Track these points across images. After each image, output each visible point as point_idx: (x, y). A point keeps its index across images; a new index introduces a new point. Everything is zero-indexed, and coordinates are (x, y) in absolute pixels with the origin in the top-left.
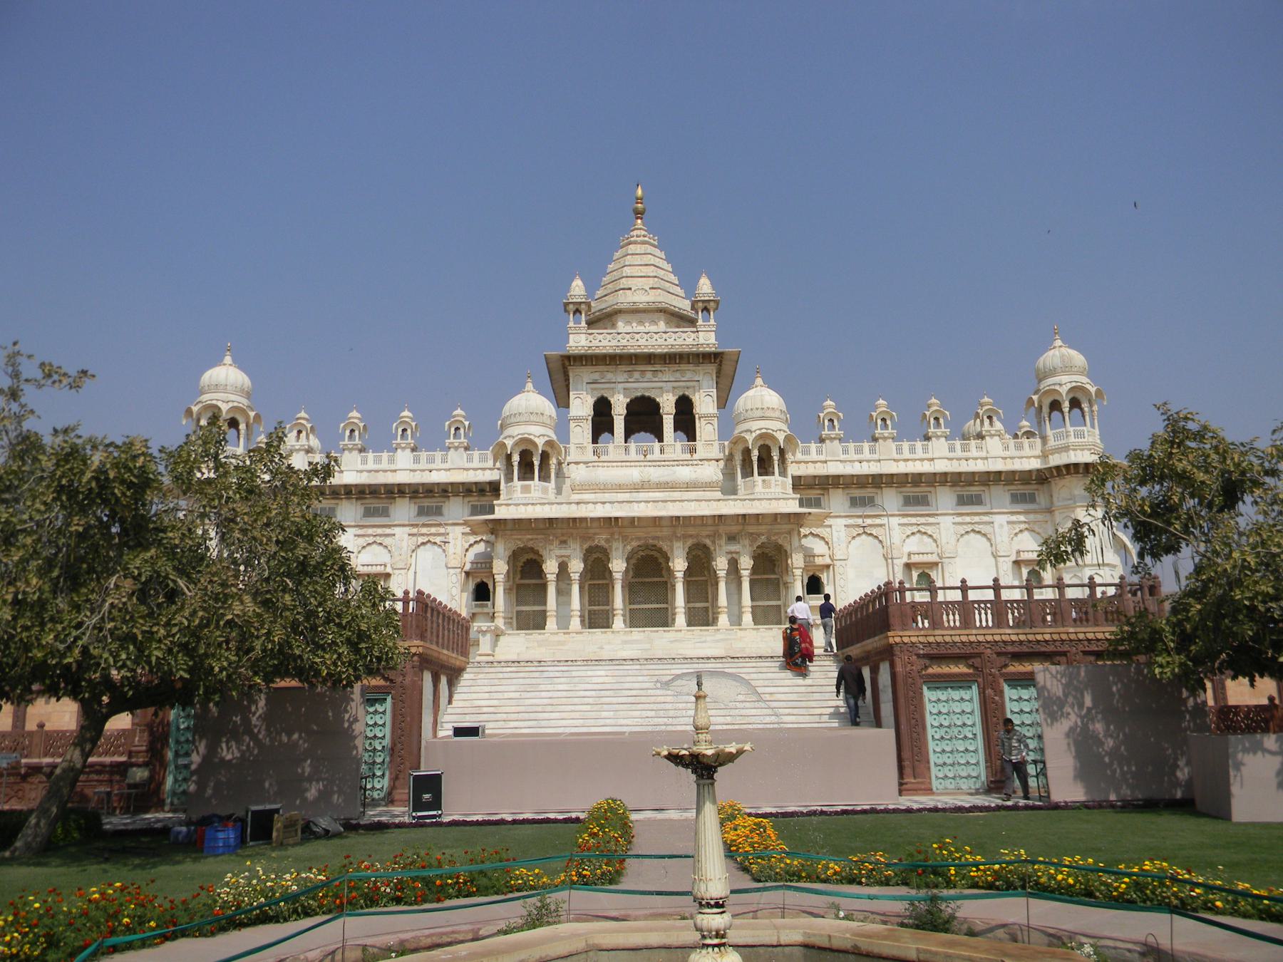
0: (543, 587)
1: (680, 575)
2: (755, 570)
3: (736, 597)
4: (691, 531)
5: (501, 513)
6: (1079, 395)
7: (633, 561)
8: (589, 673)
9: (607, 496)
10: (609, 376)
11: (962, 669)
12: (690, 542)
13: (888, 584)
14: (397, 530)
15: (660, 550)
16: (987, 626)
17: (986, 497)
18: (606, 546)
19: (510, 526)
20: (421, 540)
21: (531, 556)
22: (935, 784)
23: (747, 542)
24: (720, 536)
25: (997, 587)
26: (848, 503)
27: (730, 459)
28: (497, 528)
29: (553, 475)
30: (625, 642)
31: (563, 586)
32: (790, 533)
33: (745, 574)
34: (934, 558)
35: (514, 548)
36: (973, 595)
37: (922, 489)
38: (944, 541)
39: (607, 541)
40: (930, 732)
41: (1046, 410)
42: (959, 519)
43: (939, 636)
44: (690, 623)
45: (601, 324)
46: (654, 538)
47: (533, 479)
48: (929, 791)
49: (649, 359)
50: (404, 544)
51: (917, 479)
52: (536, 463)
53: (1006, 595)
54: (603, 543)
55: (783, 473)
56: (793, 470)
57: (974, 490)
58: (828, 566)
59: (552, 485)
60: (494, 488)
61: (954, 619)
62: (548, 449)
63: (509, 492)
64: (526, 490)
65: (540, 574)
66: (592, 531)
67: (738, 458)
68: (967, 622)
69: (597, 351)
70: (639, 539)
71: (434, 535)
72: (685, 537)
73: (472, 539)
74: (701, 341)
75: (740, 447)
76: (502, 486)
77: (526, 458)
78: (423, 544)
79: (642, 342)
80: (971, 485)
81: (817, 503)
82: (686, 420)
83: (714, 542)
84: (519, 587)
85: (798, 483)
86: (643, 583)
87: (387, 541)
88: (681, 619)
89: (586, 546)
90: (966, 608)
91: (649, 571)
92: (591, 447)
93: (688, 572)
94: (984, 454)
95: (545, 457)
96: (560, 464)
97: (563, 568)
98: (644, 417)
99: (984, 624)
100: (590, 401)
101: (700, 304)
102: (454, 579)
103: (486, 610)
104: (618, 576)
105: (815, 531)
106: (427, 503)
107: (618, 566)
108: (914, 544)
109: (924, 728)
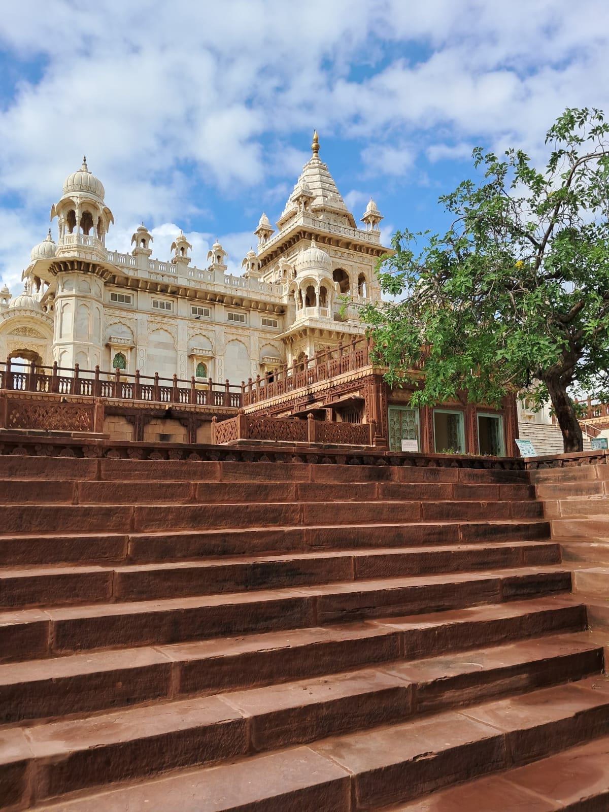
14: (217, 328)
20: (232, 337)
50: (223, 338)
87: (211, 335)
106: (235, 312)
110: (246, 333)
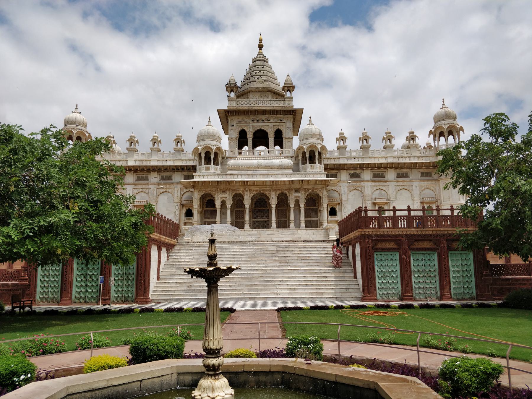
0: (216, 211)
1: (274, 206)
2: (307, 204)
3: (298, 216)
4: (279, 188)
5: (196, 179)
6: (452, 129)
7: (255, 200)
8: (231, 247)
9: (243, 172)
10: (246, 120)
11: (392, 245)
12: (278, 192)
13: (360, 208)
14: (152, 186)
15: (266, 196)
16: (404, 228)
17: (410, 174)
18: (242, 193)
19: (200, 184)
20: (162, 190)
21: (211, 198)
22: (378, 297)
23: (303, 192)
24: (291, 190)
25: (409, 210)
26: (348, 177)
27: (297, 157)
28: (195, 185)
29: (220, 163)
30: (250, 235)
31: (223, 210)
32: (322, 188)
33: (302, 206)
34: (385, 201)
35: (202, 194)
36: (398, 213)
37: (382, 170)
38: (390, 193)
39: (243, 191)
40: (377, 274)
41: (437, 135)
42: (398, 184)
43: (382, 231)
44: (278, 227)
45: (243, 97)
46: (263, 190)
47: (211, 164)
48: (376, 300)
49: (263, 112)
50: (155, 192)
51: (380, 166)
52: (212, 157)
53: (412, 213)
54: (241, 192)
55: (320, 163)
56: (325, 162)
57: (405, 171)
58: (339, 204)
59: (219, 167)
60: (194, 169)
61: (388, 224)
62: (218, 151)
63: (200, 170)
64: (208, 169)
65: (214, 205)
66: (236, 187)
67: (300, 156)
68: (395, 225)
69: (241, 108)
70: (257, 190)
71: (168, 188)
72: (276, 190)
73: (185, 190)
74: (286, 105)
75: (301, 151)
76: (198, 167)
77: (207, 154)
78: (163, 192)
79: (260, 105)
80: (402, 169)
81: (335, 176)
82: (279, 140)
83: (289, 192)
84: (205, 211)
85: (326, 168)
86: (259, 210)
88: (274, 225)
89: (234, 193)
90: (395, 219)
91: (261, 204)
92: (237, 150)
93: (278, 205)
94: (409, 156)
95: (216, 154)
96: (223, 158)
97: (223, 203)
98: (261, 138)
99: (403, 226)
100: (238, 131)
101: (286, 88)
102: (177, 208)
103: (190, 221)
104: (247, 206)
105: (333, 188)
106: (165, 174)
107: (247, 203)
108: (376, 194)
109: (374, 272)
110: (172, 186)
